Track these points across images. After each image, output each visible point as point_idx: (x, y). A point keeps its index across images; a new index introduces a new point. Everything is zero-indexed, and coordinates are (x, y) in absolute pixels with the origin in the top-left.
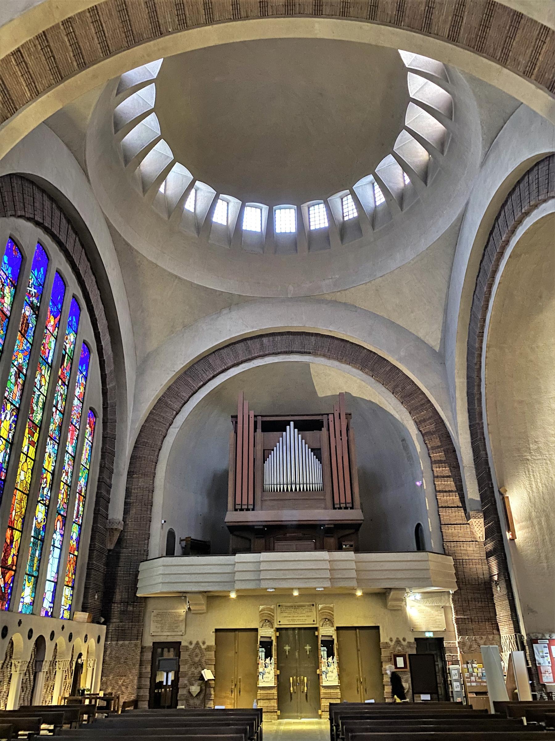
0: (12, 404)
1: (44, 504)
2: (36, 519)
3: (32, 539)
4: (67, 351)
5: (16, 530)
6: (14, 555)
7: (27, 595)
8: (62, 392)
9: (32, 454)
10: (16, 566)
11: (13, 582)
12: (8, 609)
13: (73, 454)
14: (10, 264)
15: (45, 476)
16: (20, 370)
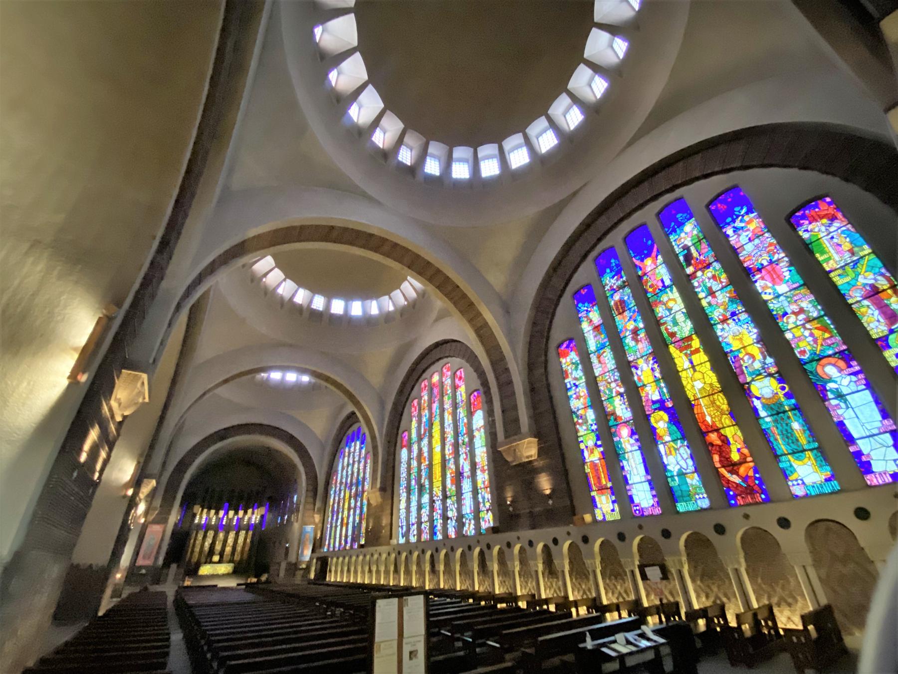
0: (642, 357)
1: (770, 375)
2: (758, 398)
3: (768, 419)
4: (690, 244)
5: (724, 428)
6: (739, 450)
7: (807, 474)
8: (710, 275)
9: (701, 358)
10: (751, 456)
11: (756, 471)
12: (767, 500)
13: (795, 286)
14: (583, 303)
15: (741, 356)
16: (635, 332)
